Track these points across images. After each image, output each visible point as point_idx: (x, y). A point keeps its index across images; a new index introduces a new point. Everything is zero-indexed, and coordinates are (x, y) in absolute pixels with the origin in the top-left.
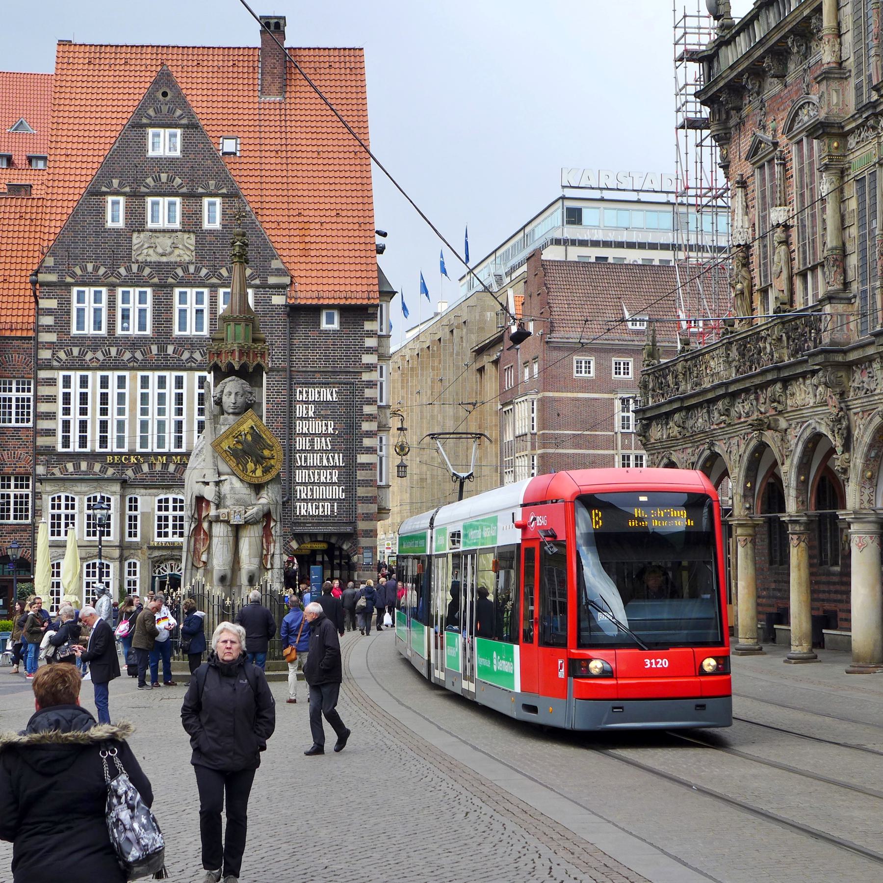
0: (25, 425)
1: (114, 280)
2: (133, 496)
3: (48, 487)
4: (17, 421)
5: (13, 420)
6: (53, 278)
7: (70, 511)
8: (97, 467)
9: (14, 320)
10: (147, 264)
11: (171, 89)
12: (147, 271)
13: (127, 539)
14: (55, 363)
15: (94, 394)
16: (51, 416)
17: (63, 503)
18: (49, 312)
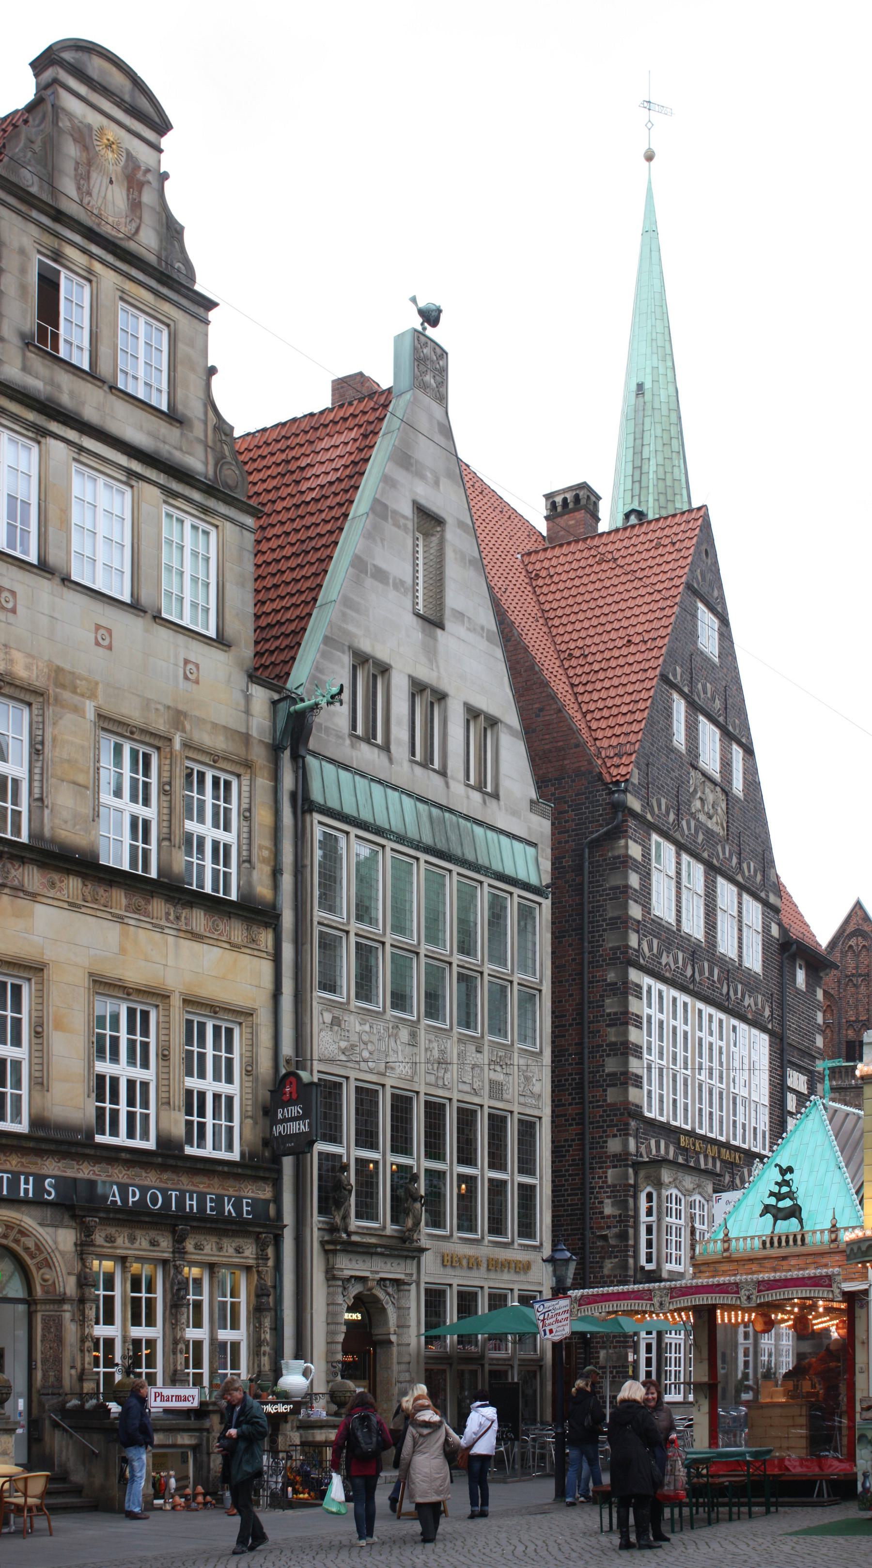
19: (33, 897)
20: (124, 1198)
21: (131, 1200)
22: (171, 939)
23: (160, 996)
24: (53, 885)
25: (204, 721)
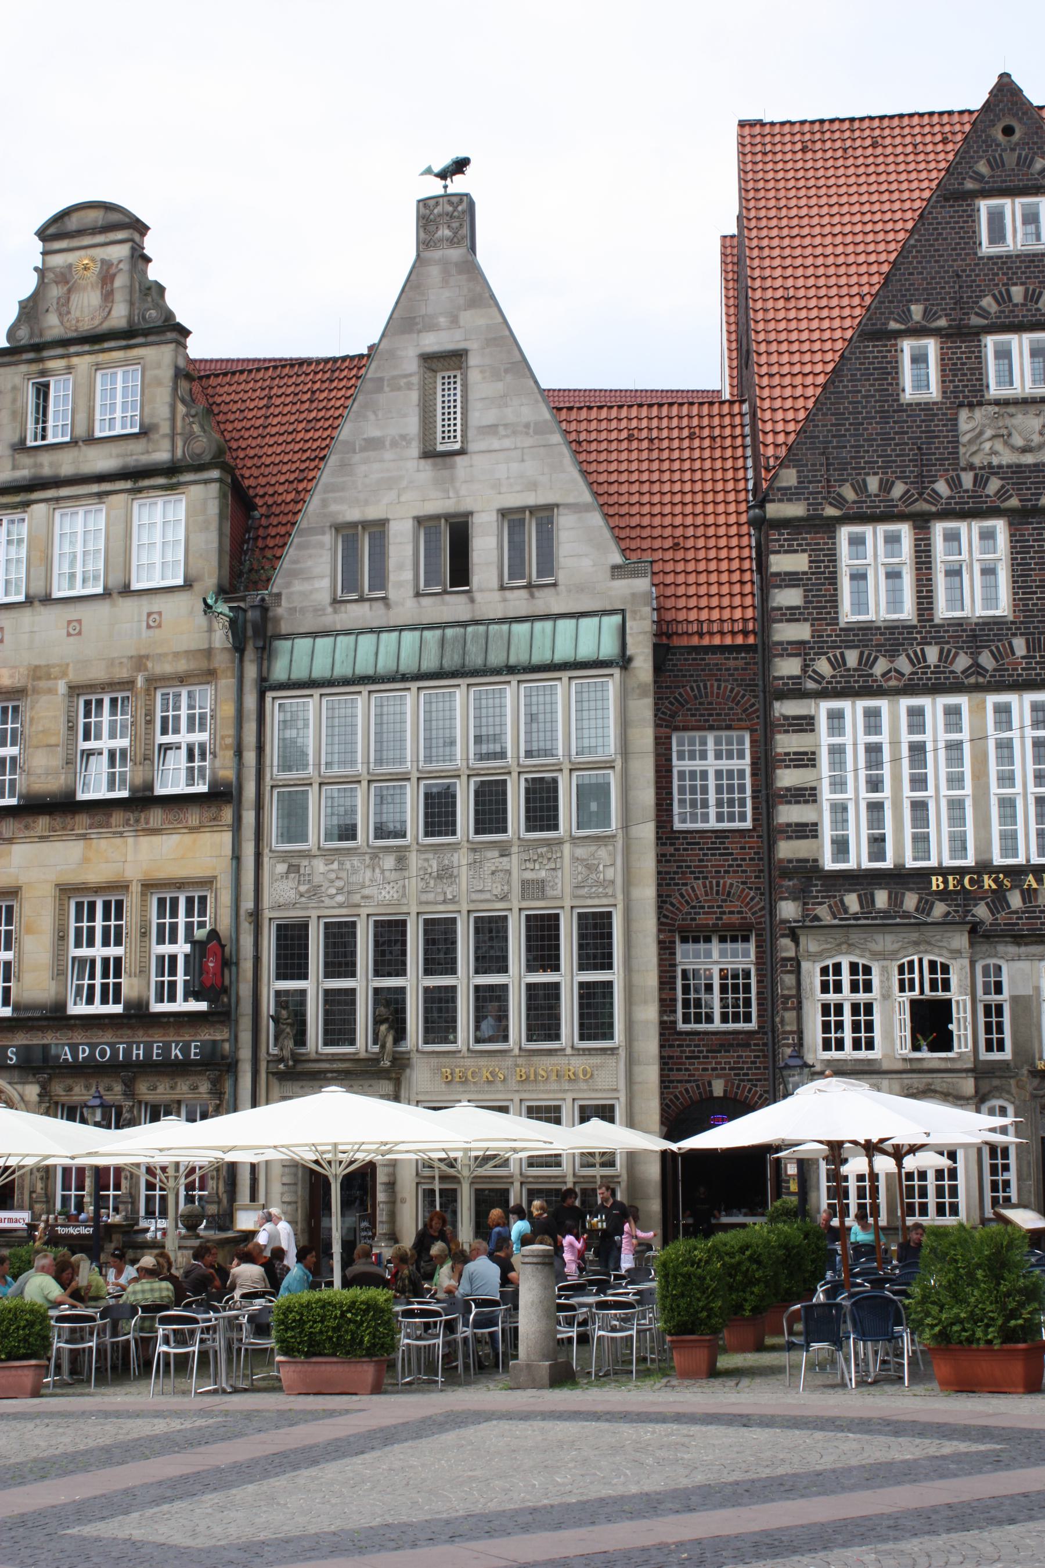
0: (737, 825)
1: (926, 507)
2: (992, 961)
3: (810, 944)
4: (720, 818)
5: (712, 816)
6: (795, 510)
7: (862, 997)
8: (910, 901)
9: (704, 615)
10: (993, 470)
11: (1020, 120)
12: (994, 485)
13: (985, 1056)
14: (811, 685)
15: (895, 743)
16: (807, 795)
17: (846, 978)
18: (791, 579)
19: (10, 841)
20: (75, 1055)
21: (81, 1056)
22: (130, 840)
23: (123, 887)
24: (27, 827)
25: (165, 655)
